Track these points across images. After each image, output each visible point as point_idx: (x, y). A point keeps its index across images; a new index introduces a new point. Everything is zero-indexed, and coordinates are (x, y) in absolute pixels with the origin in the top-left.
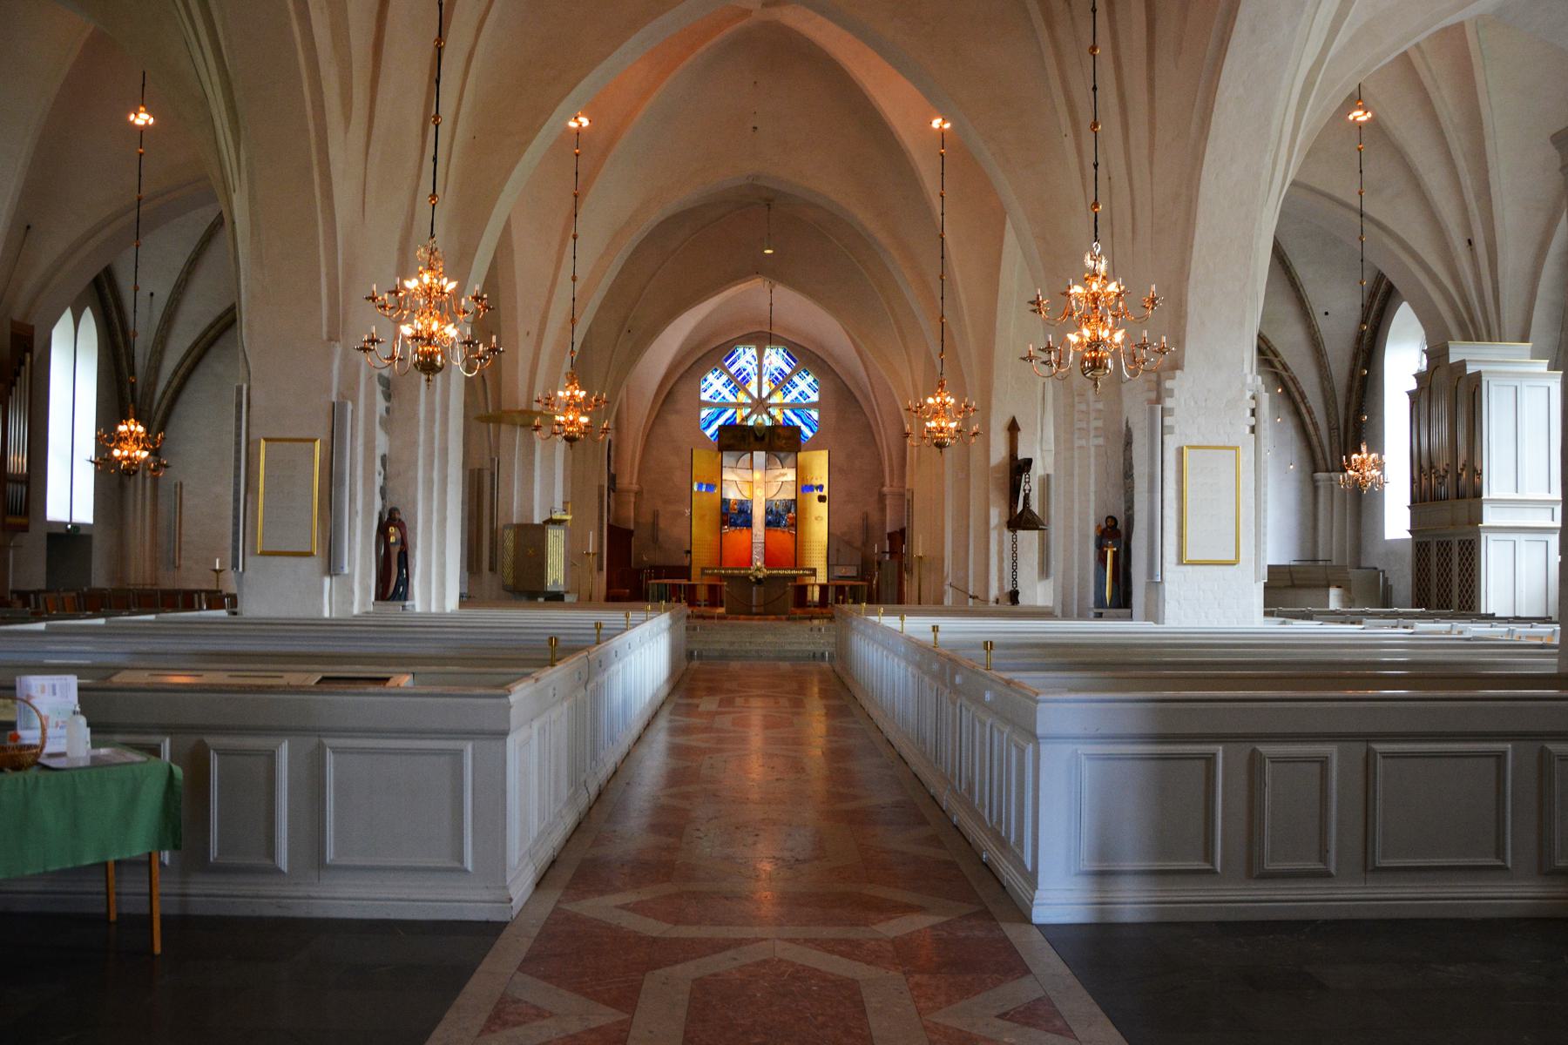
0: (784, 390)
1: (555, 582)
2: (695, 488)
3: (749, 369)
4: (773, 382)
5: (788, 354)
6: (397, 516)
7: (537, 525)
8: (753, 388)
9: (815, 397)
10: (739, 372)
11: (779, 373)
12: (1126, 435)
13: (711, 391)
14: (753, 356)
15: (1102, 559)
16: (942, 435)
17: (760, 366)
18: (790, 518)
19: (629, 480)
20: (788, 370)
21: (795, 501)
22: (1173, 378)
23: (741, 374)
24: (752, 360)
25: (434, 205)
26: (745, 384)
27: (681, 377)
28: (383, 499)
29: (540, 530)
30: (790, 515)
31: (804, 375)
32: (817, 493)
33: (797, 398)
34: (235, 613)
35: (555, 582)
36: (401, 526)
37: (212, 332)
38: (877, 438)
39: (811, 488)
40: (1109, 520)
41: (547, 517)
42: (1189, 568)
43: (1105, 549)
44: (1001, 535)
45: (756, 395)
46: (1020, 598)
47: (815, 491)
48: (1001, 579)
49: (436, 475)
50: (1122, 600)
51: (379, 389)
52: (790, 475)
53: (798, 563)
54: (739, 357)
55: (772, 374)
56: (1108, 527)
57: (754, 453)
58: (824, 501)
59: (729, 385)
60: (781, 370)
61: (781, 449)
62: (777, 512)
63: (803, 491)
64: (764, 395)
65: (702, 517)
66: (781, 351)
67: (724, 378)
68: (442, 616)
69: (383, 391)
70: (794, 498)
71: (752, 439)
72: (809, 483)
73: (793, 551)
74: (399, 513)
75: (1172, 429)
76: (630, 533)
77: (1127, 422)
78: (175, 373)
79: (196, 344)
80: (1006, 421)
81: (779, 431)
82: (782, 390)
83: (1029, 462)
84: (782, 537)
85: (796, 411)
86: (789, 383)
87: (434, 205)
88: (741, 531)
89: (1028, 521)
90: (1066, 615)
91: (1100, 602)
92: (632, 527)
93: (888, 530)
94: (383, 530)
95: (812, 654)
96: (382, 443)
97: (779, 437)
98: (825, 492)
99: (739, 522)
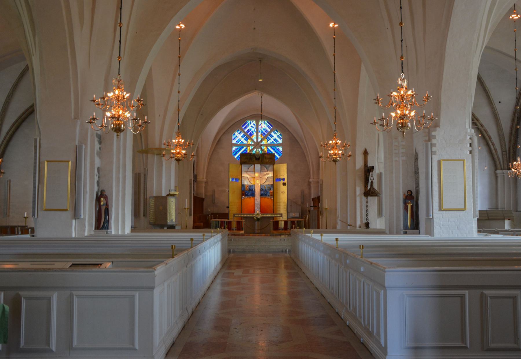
0: (268, 138)
1: (172, 220)
2: (231, 180)
3: (253, 130)
4: (263, 135)
5: (269, 123)
6: (104, 193)
7: (164, 197)
8: (254, 138)
9: (280, 141)
10: (248, 131)
11: (265, 131)
12: (415, 156)
13: (237, 139)
14: (254, 124)
15: (406, 208)
16: (336, 156)
17: (257, 128)
18: (271, 192)
19: (202, 177)
20: (269, 130)
21: (273, 185)
22: (435, 131)
23: (249, 132)
24: (254, 127)
25: (120, 61)
26: (251, 136)
27: (224, 133)
28: (98, 186)
29: (165, 198)
30: (271, 191)
31: (276, 132)
32: (282, 182)
33: (273, 142)
34: (33, 236)
35: (172, 220)
36: (106, 198)
37: (24, 116)
38: (307, 159)
40: (409, 192)
41: (168, 193)
42: (444, 212)
43: (407, 204)
44: (361, 199)
45: (255, 140)
46: (370, 225)
47: (281, 181)
48: (361, 217)
49: (121, 176)
50: (415, 226)
51: (96, 139)
52: (271, 175)
53: (274, 211)
54: (248, 125)
55: (262, 132)
56: (408, 195)
57: (256, 165)
58: (285, 185)
59: (244, 137)
60: (266, 130)
61: (267, 163)
62: (265, 190)
63: (276, 181)
64: (259, 140)
66: (266, 122)
67: (242, 134)
68: (123, 236)
69: (98, 140)
70: (272, 183)
71: (254, 159)
72: (279, 178)
74: (105, 192)
75: (435, 153)
76: (203, 200)
77: (416, 151)
78: (8, 133)
79: (16, 121)
80: (362, 150)
81: (266, 155)
82: (266, 138)
83: (372, 168)
84: (267, 200)
85: (273, 147)
86: (269, 136)
87: (120, 61)
88: (250, 198)
89: (373, 193)
90: (391, 233)
91: (406, 227)
92: (204, 197)
93: (312, 197)
94: (98, 199)
95: (281, 251)
96: (98, 162)
97: (266, 158)
98: (286, 181)
99: (249, 194)
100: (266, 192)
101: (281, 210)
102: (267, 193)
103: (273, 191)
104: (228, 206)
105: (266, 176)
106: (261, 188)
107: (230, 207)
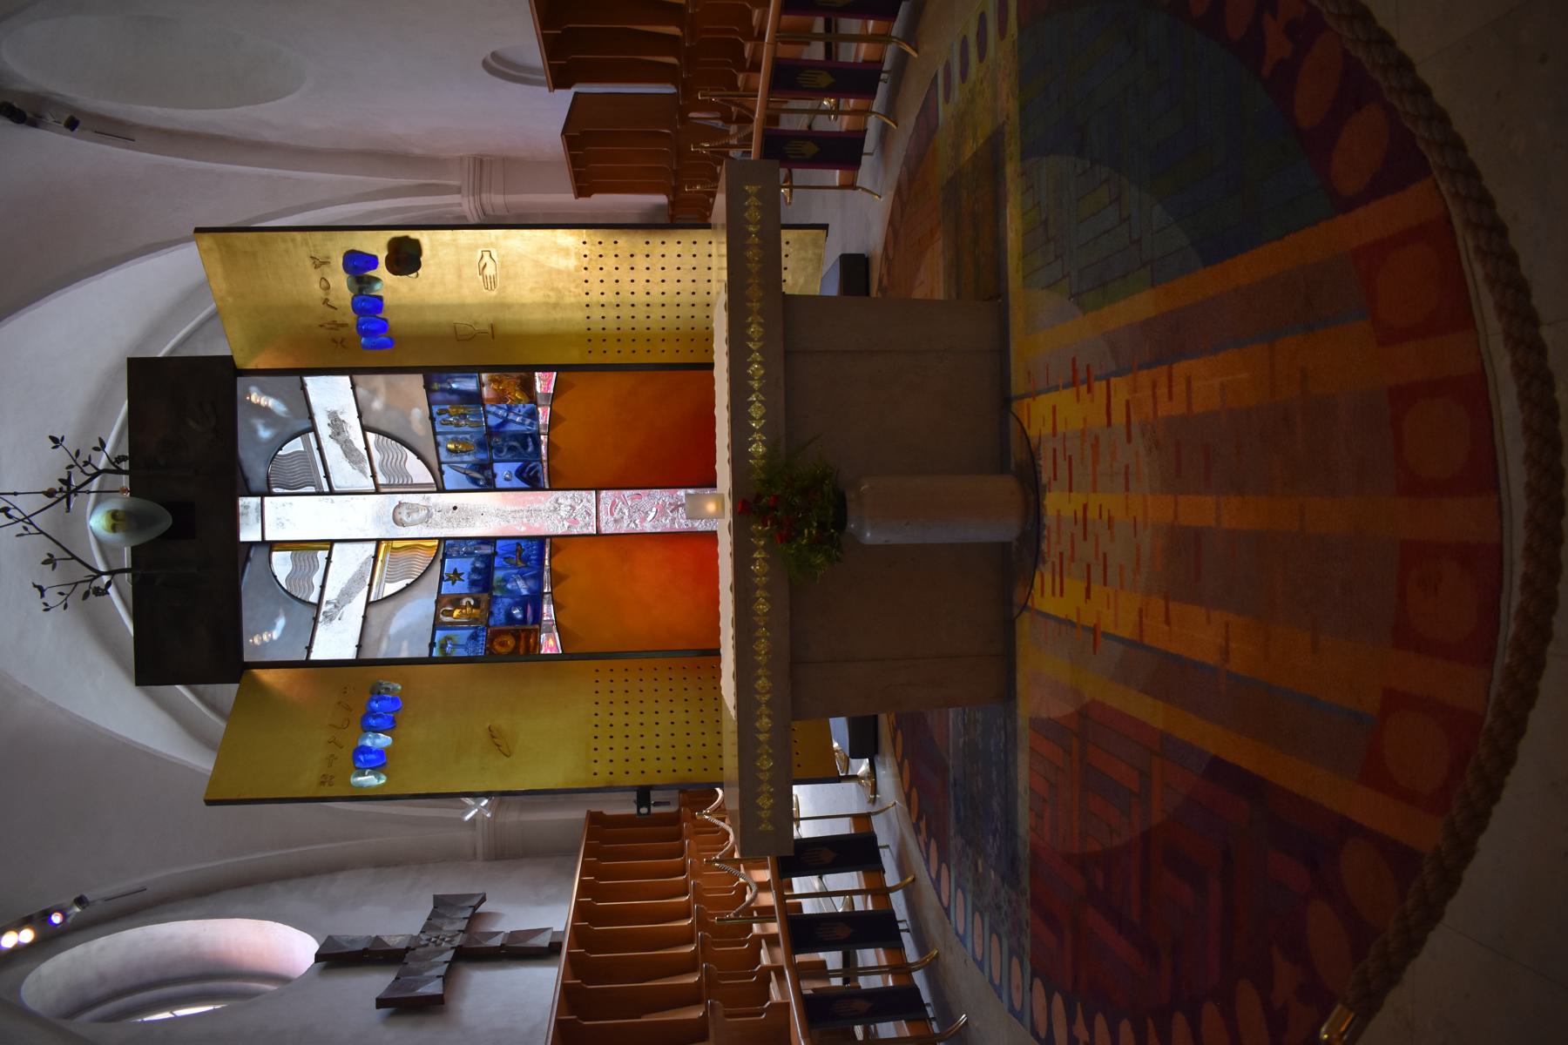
2: (370, 780)
21: (433, 376)
30: (486, 392)
32: (388, 284)
39: (369, 306)
47: (378, 290)
58: (416, 245)
62: (482, 445)
63: (390, 344)
65: (499, 743)
70: (417, 381)
72: (350, 318)
73: (626, 380)
99: (523, 588)
100: (497, 440)
101: (656, 298)
102: (512, 428)
103: (484, 377)
104: (634, 796)
105: (359, 444)
106: (474, 481)
107: (641, 781)
